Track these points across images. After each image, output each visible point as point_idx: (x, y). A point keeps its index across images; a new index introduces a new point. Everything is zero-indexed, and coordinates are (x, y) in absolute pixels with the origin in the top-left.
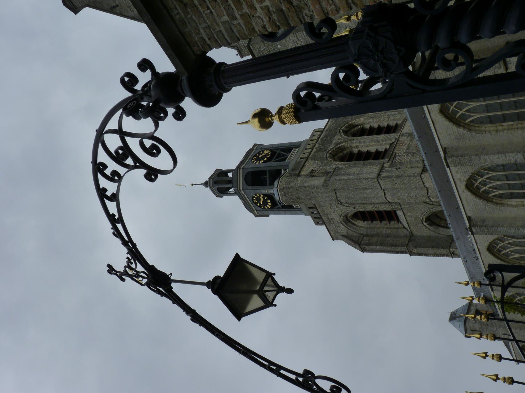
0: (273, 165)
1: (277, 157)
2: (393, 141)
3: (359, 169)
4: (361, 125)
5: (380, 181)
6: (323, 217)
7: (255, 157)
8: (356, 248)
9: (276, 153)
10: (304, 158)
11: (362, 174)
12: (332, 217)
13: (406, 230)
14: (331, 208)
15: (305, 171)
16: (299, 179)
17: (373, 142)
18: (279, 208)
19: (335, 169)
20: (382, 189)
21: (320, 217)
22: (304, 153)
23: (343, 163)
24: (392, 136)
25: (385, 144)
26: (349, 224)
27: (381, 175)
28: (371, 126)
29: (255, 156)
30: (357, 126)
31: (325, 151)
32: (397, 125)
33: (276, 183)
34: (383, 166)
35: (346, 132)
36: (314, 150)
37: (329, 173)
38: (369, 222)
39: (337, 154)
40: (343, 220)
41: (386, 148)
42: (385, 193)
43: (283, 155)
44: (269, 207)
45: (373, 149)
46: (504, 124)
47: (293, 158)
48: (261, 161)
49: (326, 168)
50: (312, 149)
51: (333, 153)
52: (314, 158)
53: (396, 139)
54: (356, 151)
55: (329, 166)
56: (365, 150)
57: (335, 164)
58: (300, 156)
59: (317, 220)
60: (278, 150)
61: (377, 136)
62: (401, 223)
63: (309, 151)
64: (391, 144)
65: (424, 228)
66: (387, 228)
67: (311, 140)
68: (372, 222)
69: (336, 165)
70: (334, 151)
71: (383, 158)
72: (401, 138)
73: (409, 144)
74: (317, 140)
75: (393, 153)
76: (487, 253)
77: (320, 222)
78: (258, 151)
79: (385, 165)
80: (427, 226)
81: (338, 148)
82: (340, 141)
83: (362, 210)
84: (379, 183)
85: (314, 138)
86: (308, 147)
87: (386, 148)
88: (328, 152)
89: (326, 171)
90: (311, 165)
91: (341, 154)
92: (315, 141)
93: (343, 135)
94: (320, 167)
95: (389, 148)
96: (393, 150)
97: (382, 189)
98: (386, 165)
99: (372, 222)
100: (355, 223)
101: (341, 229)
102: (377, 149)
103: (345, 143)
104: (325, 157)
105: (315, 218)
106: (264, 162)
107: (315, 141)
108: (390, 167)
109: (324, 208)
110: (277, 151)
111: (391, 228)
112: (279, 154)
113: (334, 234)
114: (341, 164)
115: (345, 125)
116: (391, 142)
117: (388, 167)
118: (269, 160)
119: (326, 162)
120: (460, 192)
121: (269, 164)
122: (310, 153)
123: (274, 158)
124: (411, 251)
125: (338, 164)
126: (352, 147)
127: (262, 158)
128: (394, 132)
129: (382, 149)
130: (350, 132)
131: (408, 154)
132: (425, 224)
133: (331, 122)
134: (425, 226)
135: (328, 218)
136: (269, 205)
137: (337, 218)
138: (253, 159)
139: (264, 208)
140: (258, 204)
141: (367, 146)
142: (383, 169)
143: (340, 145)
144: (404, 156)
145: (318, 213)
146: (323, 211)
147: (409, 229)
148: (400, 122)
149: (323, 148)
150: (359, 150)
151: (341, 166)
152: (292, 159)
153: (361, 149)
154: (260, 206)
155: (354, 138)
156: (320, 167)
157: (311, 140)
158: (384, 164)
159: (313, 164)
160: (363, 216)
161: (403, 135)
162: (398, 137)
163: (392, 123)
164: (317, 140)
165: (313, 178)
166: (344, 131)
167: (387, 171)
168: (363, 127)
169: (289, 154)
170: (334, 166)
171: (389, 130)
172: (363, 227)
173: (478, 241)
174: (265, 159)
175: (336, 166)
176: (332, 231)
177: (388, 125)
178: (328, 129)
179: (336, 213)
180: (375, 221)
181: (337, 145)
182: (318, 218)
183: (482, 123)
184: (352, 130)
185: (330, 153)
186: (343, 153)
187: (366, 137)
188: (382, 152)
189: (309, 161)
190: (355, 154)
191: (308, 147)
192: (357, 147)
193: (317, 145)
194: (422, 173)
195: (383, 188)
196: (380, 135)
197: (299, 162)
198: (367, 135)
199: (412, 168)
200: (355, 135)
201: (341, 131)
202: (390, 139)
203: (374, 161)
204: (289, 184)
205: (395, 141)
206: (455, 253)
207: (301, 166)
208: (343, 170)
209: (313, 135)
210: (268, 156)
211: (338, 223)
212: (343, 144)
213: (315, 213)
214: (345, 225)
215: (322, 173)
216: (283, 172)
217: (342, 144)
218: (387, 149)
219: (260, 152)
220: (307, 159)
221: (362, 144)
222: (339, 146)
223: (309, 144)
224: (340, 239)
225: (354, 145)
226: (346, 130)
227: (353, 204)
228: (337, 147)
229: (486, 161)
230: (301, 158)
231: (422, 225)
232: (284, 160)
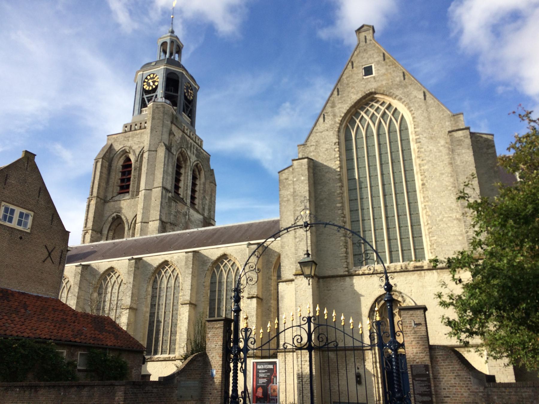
0: (181, 101)
2: (185, 201)
3: (171, 173)
4: (200, 177)
5: (160, 188)
6: (131, 133)
7: (189, 86)
8: (99, 154)
10: (184, 129)
11: (167, 175)
12: (130, 140)
13: (111, 198)
14: (139, 141)
15: (174, 128)
16: (169, 123)
18: (143, 95)
19: (173, 154)
22: (187, 130)
23: (176, 161)
24: (189, 201)
25: (183, 195)
26: (122, 153)
28: (197, 185)
29: (191, 86)
30: (199, 174)
32: (195, 204)
33: (168, 102)
35: (197, 165)
36: (188, 138)
37: (171, 149)
38: (121, 170)
42: (148, 190)
43: (187, 110)
44: (145, 87)
45: (181, 184)
46: (209, 291)
48: (185, 91)
50: (189, 137)
51: (184, 153)
52: (183, 138)
53: (186, 204)
54: (182, 171)
56: (182, 178)
59: (129, 127)
60: (192, 106)
61: (191, 190)
62: (117, 195)
63: (188, 134)
64: (183, 199)
65: (111, 213)
66: (114, 183)
67: (196, 137)
68: (120, 172)
69: (175, 155)
70: (185, 154)
71: (175, 192)
72: (186, 207)
76: (109, 266)
80: (113, 215)
81: (187, 158)
82: (191, 160)
84: (158, 187)
85: (197, 140)
89: (172, 147)
90: (178, 134)
91: (181, 159)
93: (195, 163)
94: (176, 141)
98: (170, 195)
99: (120, 172)
100: (122, 158)
104: (182, 146)
105: (131, 126)
106: (185, 93)
109: (139, 136)
111: (113, 187)
113: (114, 138)
114: (175, 159)
115: (202, 166)
116: (184, 199)
118: (186, 97)
119: (179, 147)
120: (163, 256)
121: (183, 97)
122: (187, 135)
123: (186, 103)
124: (92, 199)
126: (185, 168)
127: (188, 92)
128: (191, 202)
129: (181, 191)
130: (196, 168)
131: (176, 212)
132: (115, 214)
133: (206, 155)
134: (113, 214)
135: (129, 137)
136: (147, 87)
137: (129, 144)
138: (188, 83)
139: (144, 82)
140: (149, 77)
141: (184, 181)
145: (135, 130)
146: (137, 135)
147: (111, 200)
148: (196, 207)
150: (182, 174)
153: (183, 175)
154: (146, 78)
156: (176, 141)
157: (196, 137)
163: (197, 201)
164: (195, 142)
165: (168, 135)
166: (197, 164)
167: (166, 195)
168: (197, 179)
170: (175, 153)
171: (193, 198)
172: (117, 164)
173: (119, 261)
174: (186, 94)
176: (117, 137)
177: (196, 198)
178: (202, 152)
179: (134, 144)
180: (122, 175)
183: (212, 277)
184: (197, 170)
185: (184, 151)
188: (178, 191)
189: (181, 133)
190: (180, 170)
193: (191, 141)
200: (194, 171)
201: (198, 162)
202: (186, 199)
203: (174, 185)
204: (166, 114)
206: (87, 234)
207: (178, 126)
209: (199, 139)
210: (188, 97)
211: (124, 144)
213: (136, 127)
214: (121, 150)
216: (175, 108)
217: (189, 161)
220: (183, 132)
223: (193, 135)
225: (187, 171)
226: (198, 165)
229: (187, 277)
230: (184, 127)
231: (114, 212)
232: (184, 111)
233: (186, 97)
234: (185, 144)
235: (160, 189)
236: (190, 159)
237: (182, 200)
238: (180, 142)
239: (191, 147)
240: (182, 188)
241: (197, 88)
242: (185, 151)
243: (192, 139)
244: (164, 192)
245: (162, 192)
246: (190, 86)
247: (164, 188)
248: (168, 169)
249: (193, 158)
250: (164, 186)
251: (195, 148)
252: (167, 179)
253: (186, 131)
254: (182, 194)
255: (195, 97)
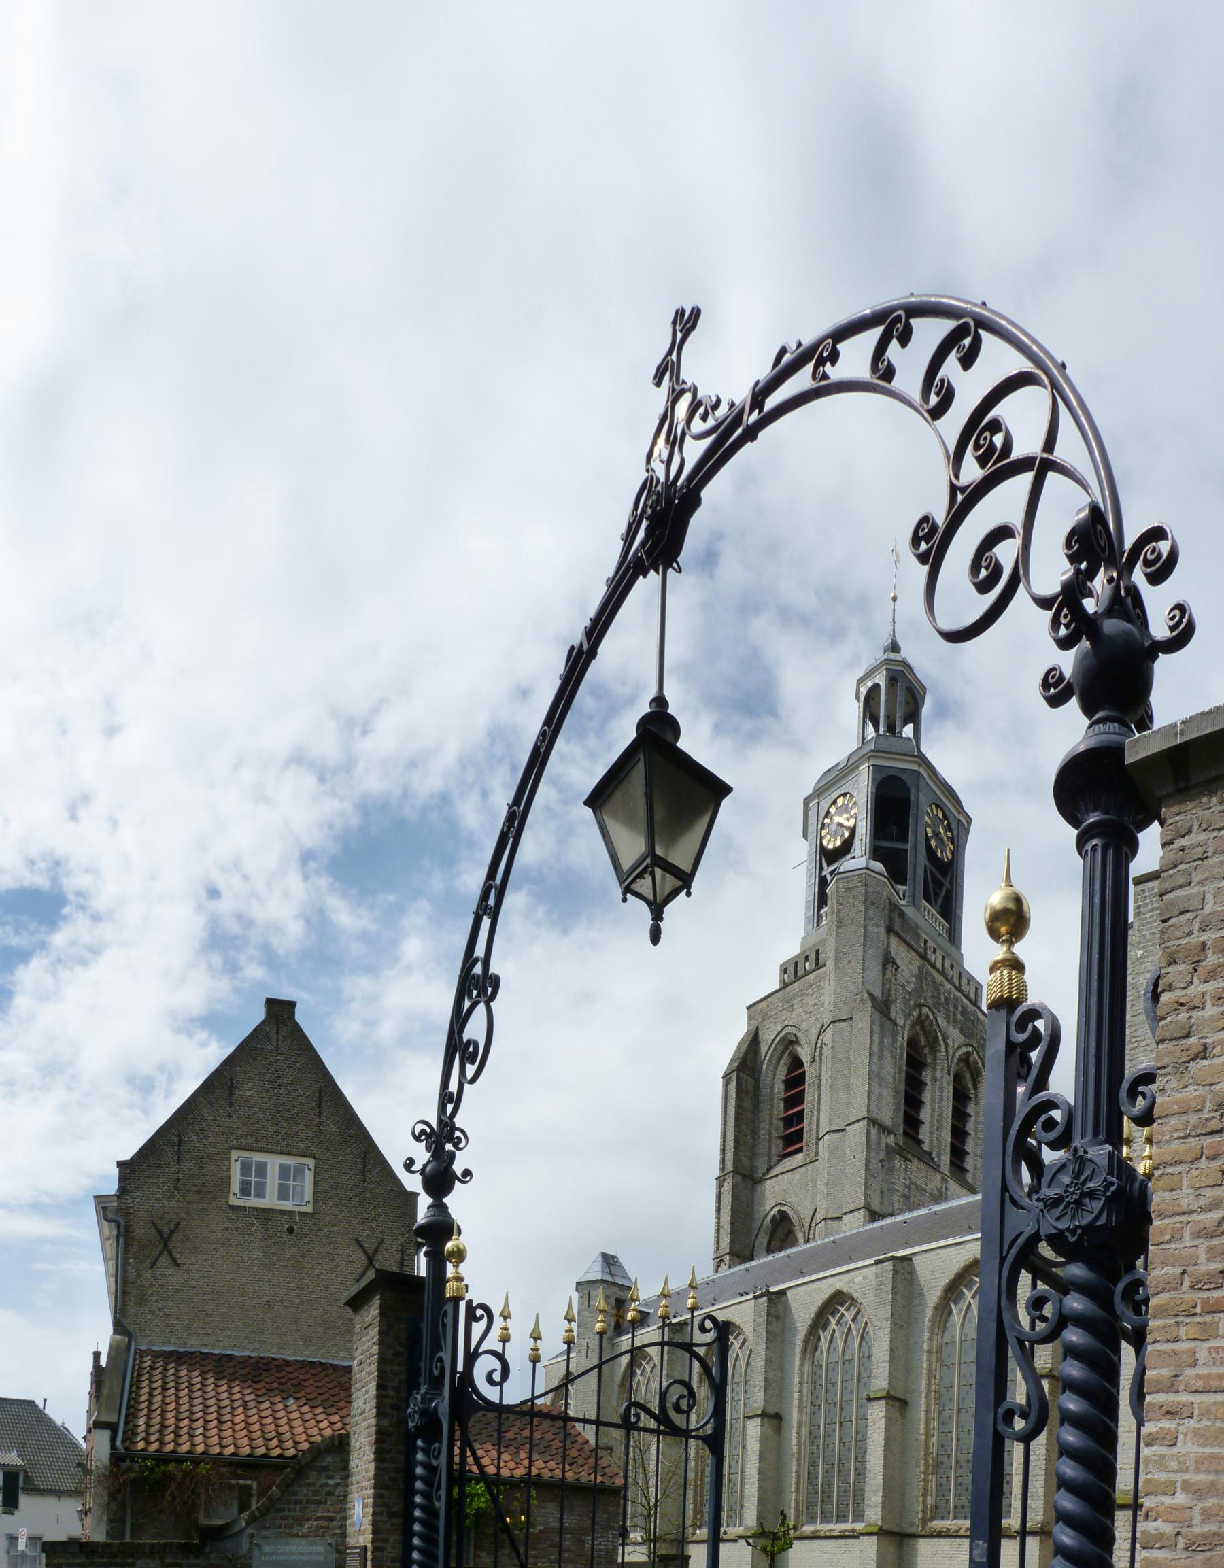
0: (917, 864)
1: (934, 878)
2: (936, 1159)
3: (890, 1079)
5: (862, 1123)
9: (944, 876)
11: (879, 1085)
17: (939, 1116)
20: (846, 1125)
21: (796, 978)
24: (945, 1159)
25: (931, 1141)
27: (874, 1126)
31: (934, 1005)
32: (964, 1171)
34: (890, 1132)
36: (940, 979)
39: (925, 1032)
40: (788, 1033)
41: (923, 1143)
43: (936, 895)
45: (925, 1114)
47: (926, 918)
49: (898, 1001)
50: (942, 973)
51: (927, 1023)
52: (921, 976)
53: (939, 1166)
54: (927, 1076)
55: (902, 1010)
56: (926, 1096)
57: (904, 1024)
58: (932, 940)
63: (939, 965)
64: (930, 1154)
69: (903, 1028)
70: (932, 1025)
71: (905, 1133)
72: (938, 1176)
73: (925, 1190)
74: (959, 989)
75: (914, 1156)
77: (786, 976)
78: (954, 826)
79: (892, 1136)
81: (937, 1037)
82: (950, 1042)
83: (807, 1078)
84: (858, 1121)
86: (947, 964)
87: (923, 1143)
88: (930, 1010)
91: (923, 1041)
92: (957, 984)
94: (903, 986)
95: (925, 1149)
96: (919, 1158)
97: (846, 1125)
98: (891, 1140)
101: (769, 1028)
102: (924, 1123)
103: (944, 1054)
107: (957, 984)
108: (887, 1146)
110: (948, 879)
112: (940, 885)
114: (902, 1040)
117: (886, 1144)
118: (931, 853)
119: (912, 1003)
123: (934, 870)
125: (903, 1033)
126: (934, 1068)
128: (952, 1163)
129: (924, 1134)
131: (908, 1187)
141: (933, 1102)
142: (884, 1132)
143: (942, 1042)
144: (905, 1179)
149: (940, 999)
150: (926, 1084)
151: (899, 1039)
152: (926, 917)
153: (929, 1087)
155: (952, 1076)
156: (903, 986)
157: (960, 974)
158: (895, 1135)
159: (910, 971)
160: (796, 1080)
161: (944, 1180)
162: (942, 1170)
163: (969, 1163)
164: (959, 989)
167: (879, 1142)
169: (938, 912)
170: (901, 1022)
171: (958, 1154)
174: (933, 843)
175: (901, 1027)
177: (968, 1153)
181: (943, 1035)
182: (796, 972)
185: (927, 1016)
186: (925, 1046)
187: (951, 1103)
191: (947, 964)
192: (934, 1080)
193: (948, 986)
194: (869, 1210)
195: (847, 1128)
196: (950, 1134)
197: (917, 936)
198: (953, 1105)
199: (882, 1192)
202: (939, 1154)
203: (901, 1114)
205: (934, 1162)
208: (890, 1041)
210: (939, 854)
212: (944, 1050)
215: (890, 990)
217: (943, 1046)
218: (922, 1146)
219: (950, 830)
221: (938, 1093)
222: (940, 1038)
223: (952, 966)
224: (749, 1024)
225: (938, 1074)
227: (820, 1059)
228: (939, 1034)
233: (931, 853)
234: (929, 994)
235: (863, 1123)
236: (944, 1040)
237: (927, 1158)
238: (915, 990)
239: (947, 999)
240: (927, 1124)
241: (964, 822)
242: (931, 1017)
243: (950, 981)
244: (874, 1132)
245: (868, 1132)
246: (944, 815)
247: (873, 1121)
248: (881, 1067)
249: (955, 1036)
250: (874, 1115)
251: (960, 1009)
252: (880, 1095)
253: (932, 957)
254: (927, 1141)
255: (958, 852)
